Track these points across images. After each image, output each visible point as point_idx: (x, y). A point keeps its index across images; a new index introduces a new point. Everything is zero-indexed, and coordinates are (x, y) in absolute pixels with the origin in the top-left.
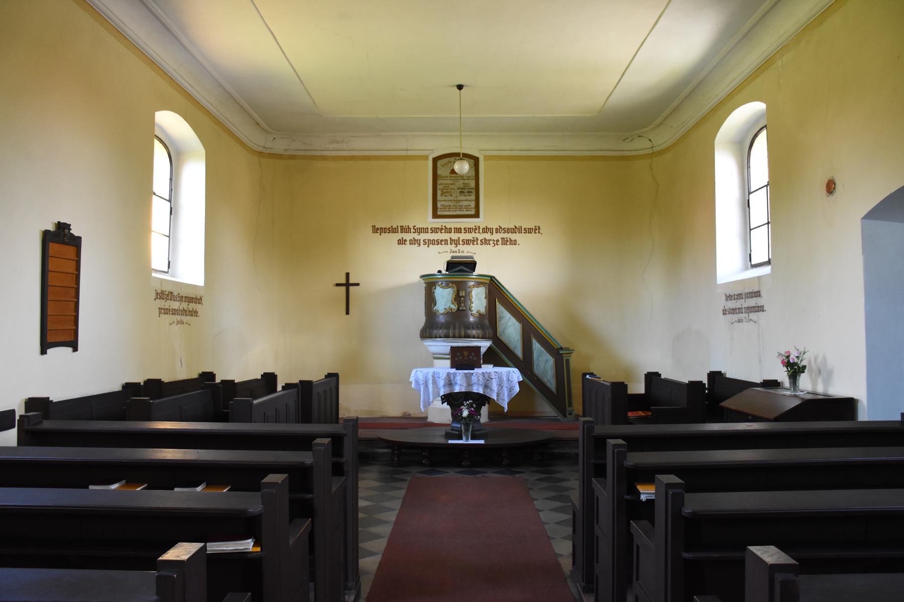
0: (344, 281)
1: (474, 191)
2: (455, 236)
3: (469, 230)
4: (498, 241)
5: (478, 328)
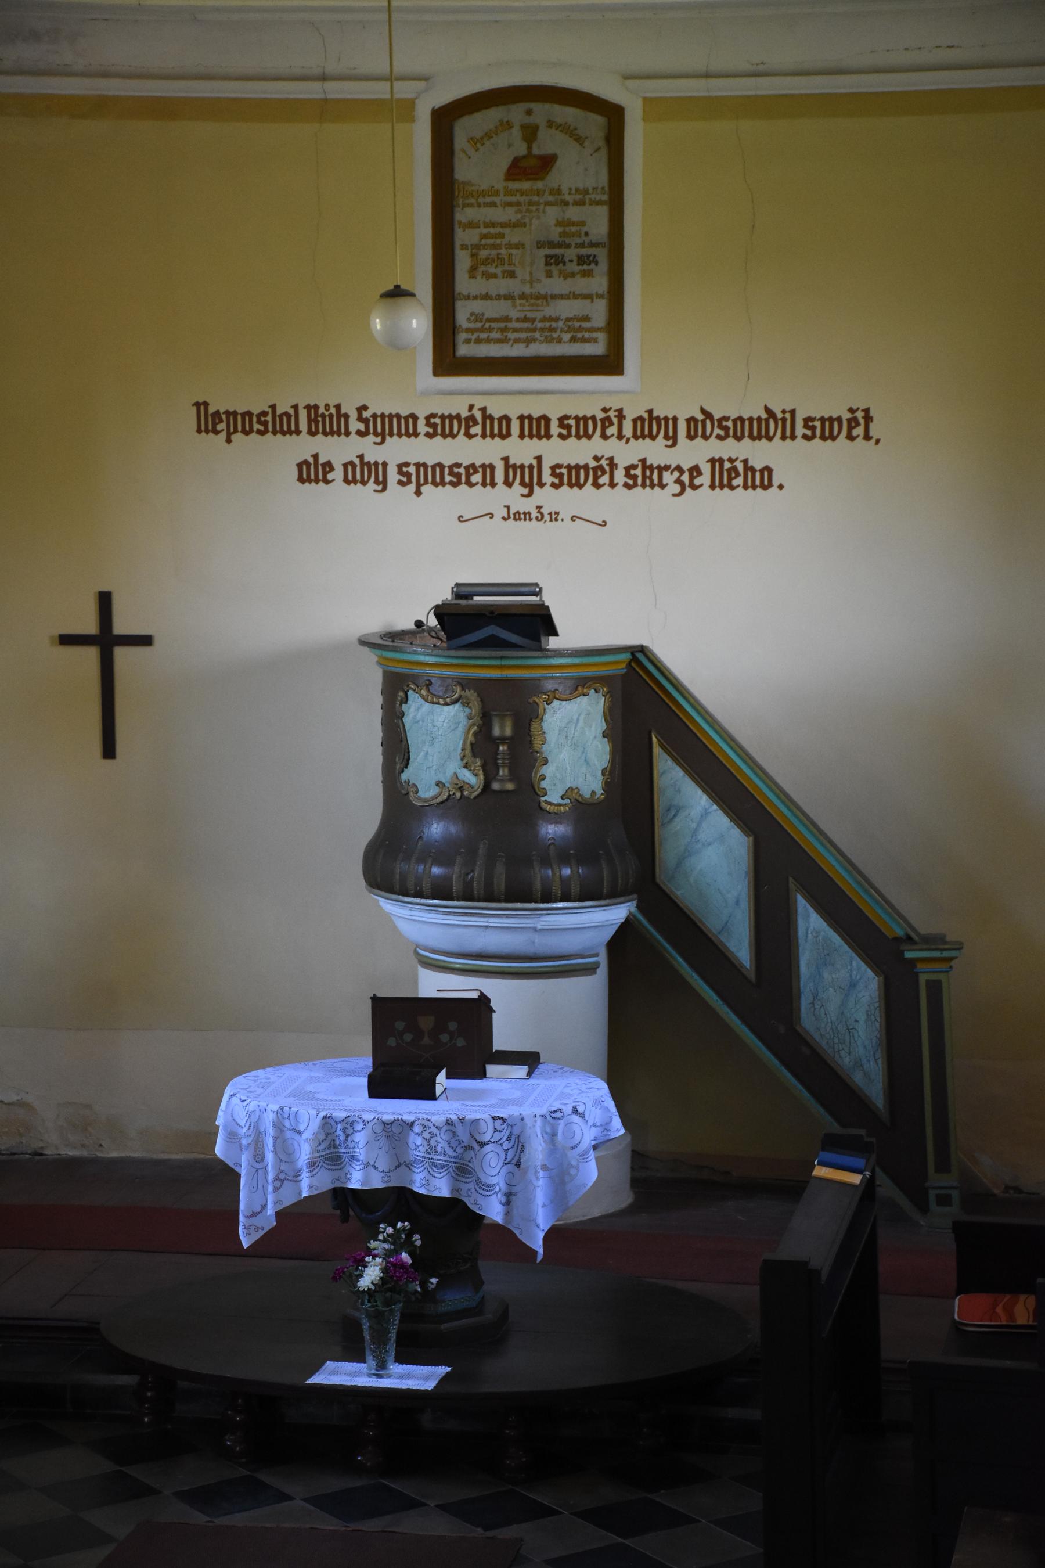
0: (90, 626)
1: (602, 254)
2: (522, 450)
3: (577, 427)
4: (695, 471)
5: (564, 859)
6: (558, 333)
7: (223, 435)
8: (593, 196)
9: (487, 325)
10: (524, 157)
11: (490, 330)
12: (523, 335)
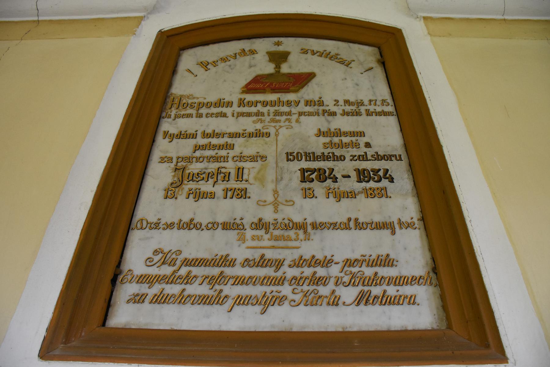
1: (399, 170)
6: (331, 286)
8: (372, 108)
9: (184, 271)
10: (271, 75)
11: (188, 279)
12: (257, 291)
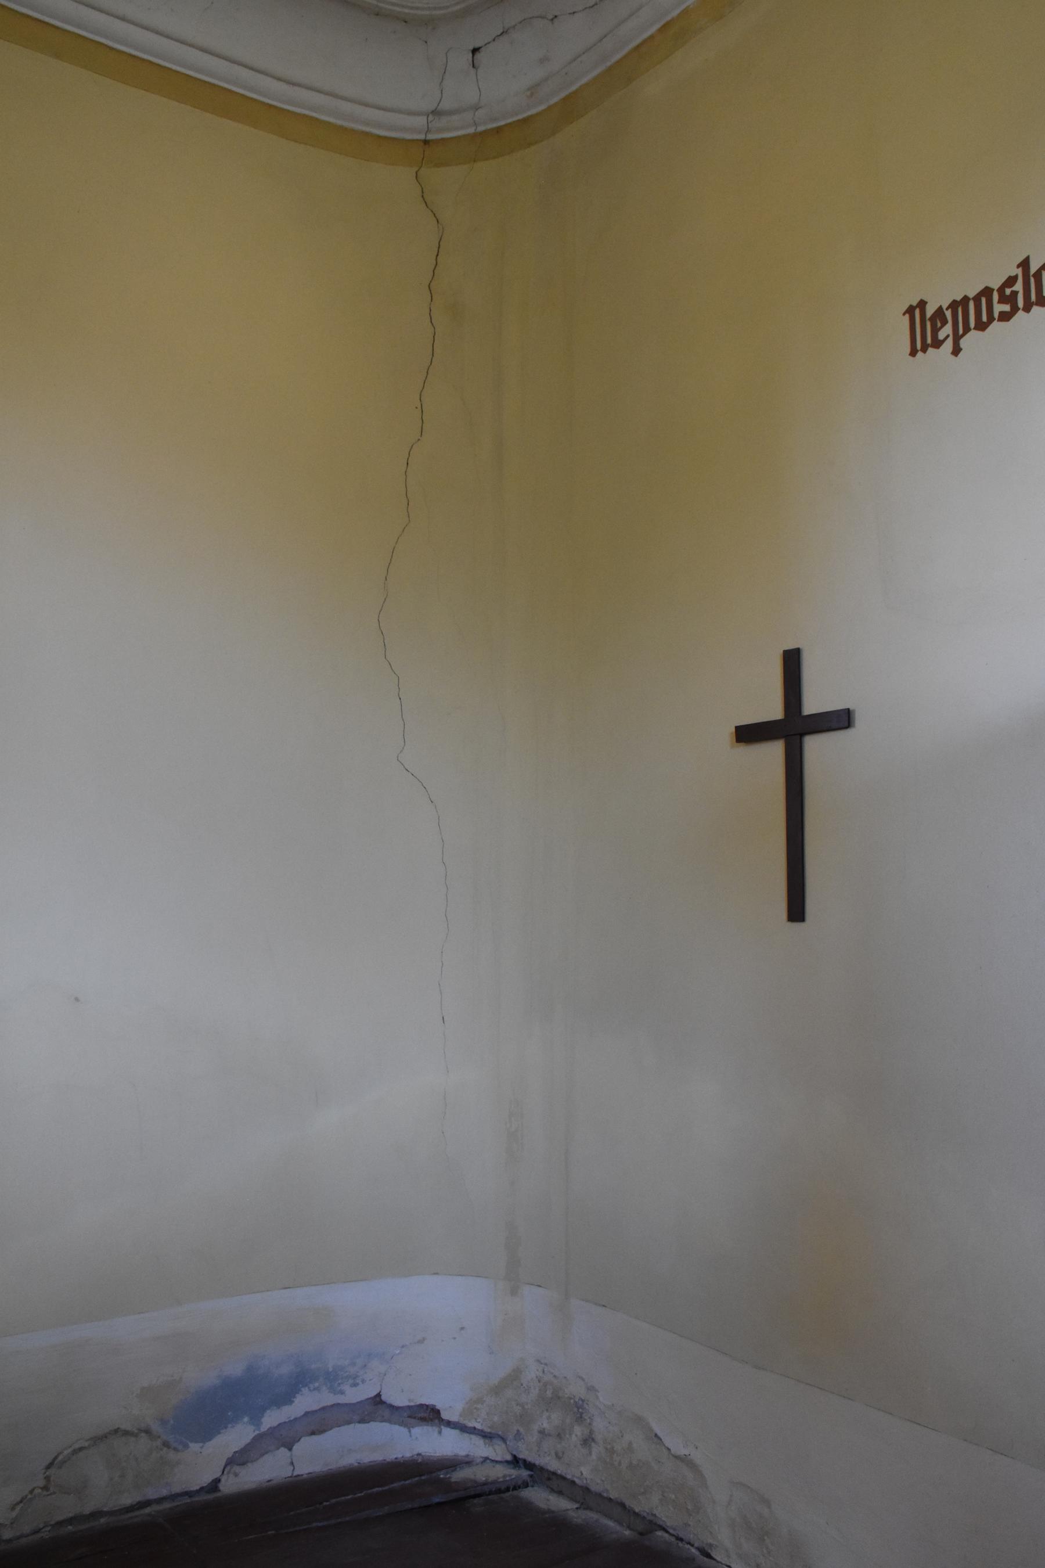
7: (948, 345)
